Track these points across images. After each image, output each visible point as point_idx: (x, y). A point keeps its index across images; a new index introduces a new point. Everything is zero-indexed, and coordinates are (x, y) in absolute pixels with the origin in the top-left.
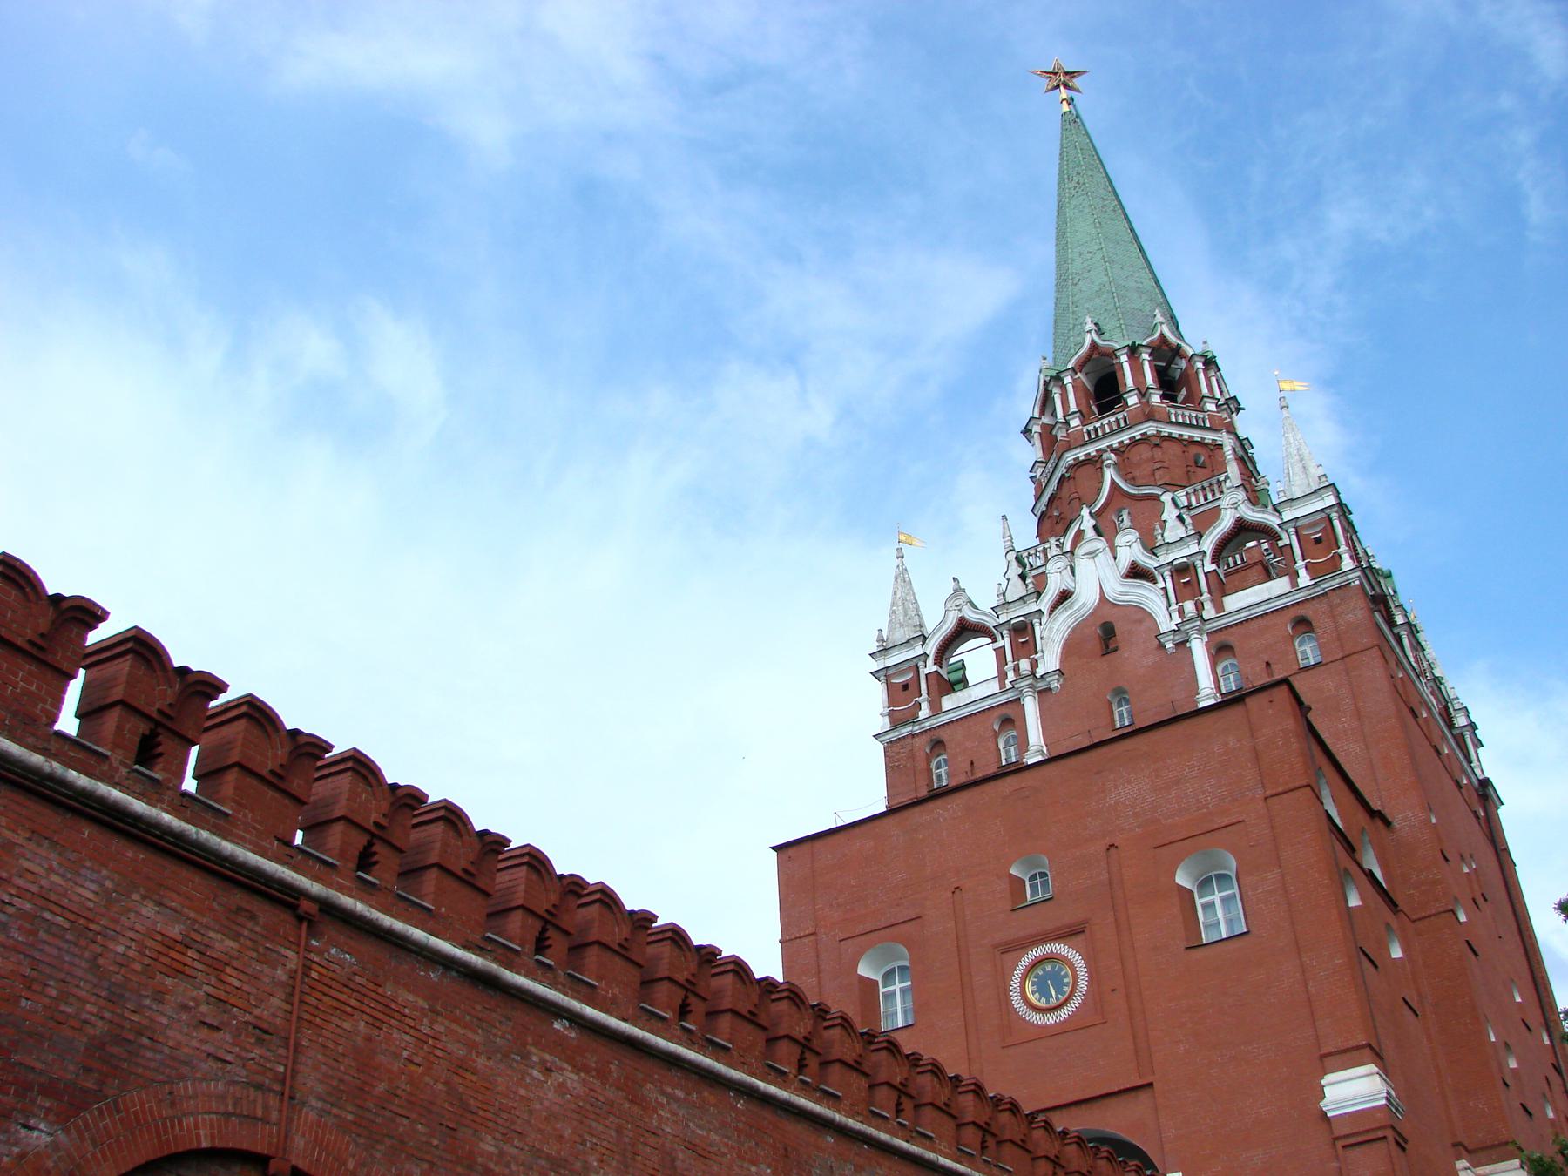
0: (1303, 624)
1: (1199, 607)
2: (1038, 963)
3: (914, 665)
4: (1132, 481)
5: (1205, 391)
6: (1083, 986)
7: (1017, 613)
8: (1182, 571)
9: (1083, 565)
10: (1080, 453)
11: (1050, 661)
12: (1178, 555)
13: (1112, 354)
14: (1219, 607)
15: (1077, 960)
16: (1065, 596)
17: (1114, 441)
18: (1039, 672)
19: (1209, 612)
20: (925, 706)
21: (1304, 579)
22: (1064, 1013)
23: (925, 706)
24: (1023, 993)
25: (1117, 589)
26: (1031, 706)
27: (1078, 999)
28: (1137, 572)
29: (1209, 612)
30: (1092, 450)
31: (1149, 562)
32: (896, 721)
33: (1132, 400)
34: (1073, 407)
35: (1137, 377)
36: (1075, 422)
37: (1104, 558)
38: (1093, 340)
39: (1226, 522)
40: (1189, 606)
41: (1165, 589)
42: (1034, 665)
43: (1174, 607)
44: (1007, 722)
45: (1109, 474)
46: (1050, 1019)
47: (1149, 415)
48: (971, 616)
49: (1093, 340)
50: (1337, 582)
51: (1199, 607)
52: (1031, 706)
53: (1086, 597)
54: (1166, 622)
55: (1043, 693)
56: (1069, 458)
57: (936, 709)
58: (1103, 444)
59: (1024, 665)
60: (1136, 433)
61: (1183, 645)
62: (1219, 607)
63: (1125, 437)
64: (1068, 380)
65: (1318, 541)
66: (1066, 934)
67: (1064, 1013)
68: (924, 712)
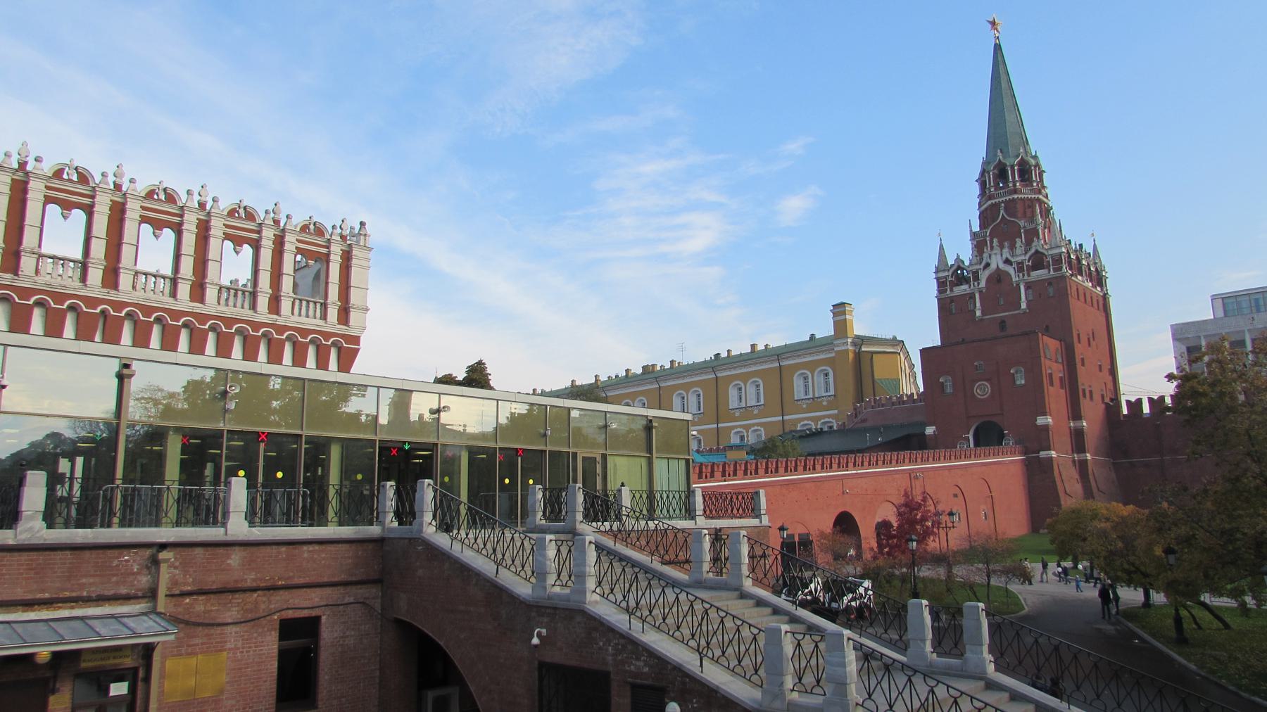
0: (1050, 284)
1: (1024, 275)
2: (978, 386)
3: (945, 277)
4: (1007, 214)
5: (1034, 179)
6: (989, 391)
7: (975, 268)
8: (1020, 265)
9: (993, 256)
10: (993, 201)
11: (983, 284)
12: (1019, 259)
13: (1005, 165)
14: (1029, 275)
15: (989, 386)
16: (988, 265)
17: (1004, 199)
18: (980, 286)
19: (1026, 277)
20: (948, 290)
21: (1052, 272)
22: (986, 396)
23: (948, 290)
24: (977, 392)
25: (1002, 266)
26: (977, 296)
27: (988, 394)
28: (1007, 262)
29: (1026, 277)
30: (997, 201)
31: (1010, 258)
32: (940, 292)
33: (1011, 185)
34: (992, 184)
35: (1014, 176)
36: (992, 190)
37: (999, 256)
38: (999, 159)
39: (1033, 251)
40: (1021, 275)
41: (1014, 268)
42: (978, 284)
43: (1017, 274)
44: (970, 298)
45: (1002, 212)
46: (982, 397)
47: (1015, 191)
48: (962, 265)
49: (999, 159)
50: (1061, 275)
51: (1024, 275)
52: (977, 296)
53: (993, 266)
54: (1015, 279)
55: (981, 292)
56: (989, 202)
57: (951, 290)
58: (1000, 200)
59: (976, 283)
60: (1011, 197)
61: (1018, 285)
62: (1029, 275)
63: (1007, 198)
64: (991, 173)
65: (1057, 260)
66: (986, 380)
67: (986, 396)
68: (948, 292)
